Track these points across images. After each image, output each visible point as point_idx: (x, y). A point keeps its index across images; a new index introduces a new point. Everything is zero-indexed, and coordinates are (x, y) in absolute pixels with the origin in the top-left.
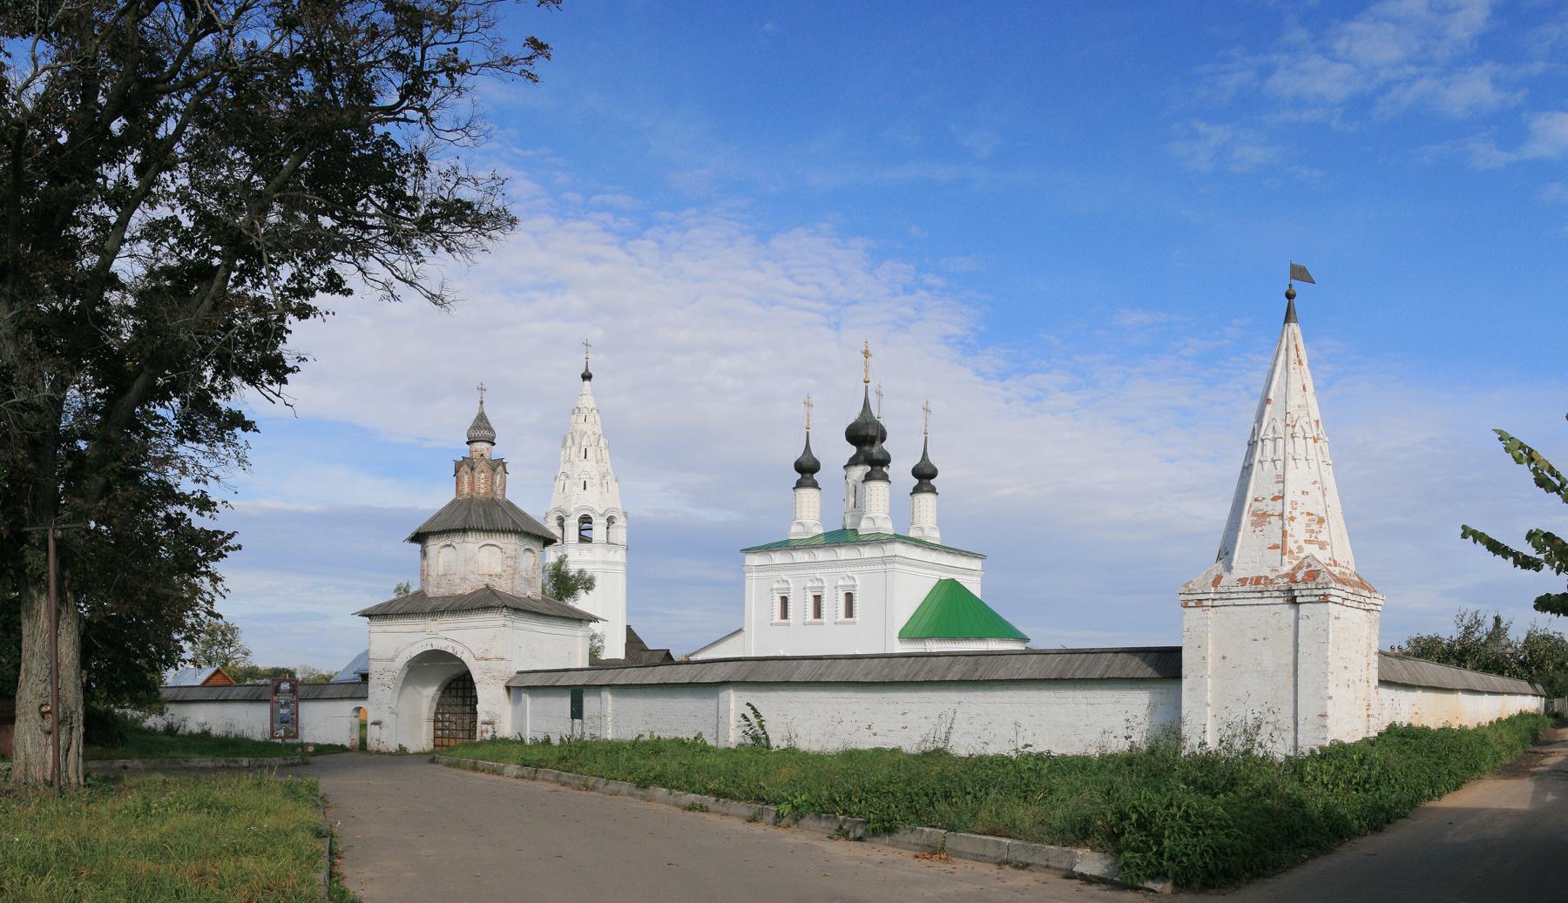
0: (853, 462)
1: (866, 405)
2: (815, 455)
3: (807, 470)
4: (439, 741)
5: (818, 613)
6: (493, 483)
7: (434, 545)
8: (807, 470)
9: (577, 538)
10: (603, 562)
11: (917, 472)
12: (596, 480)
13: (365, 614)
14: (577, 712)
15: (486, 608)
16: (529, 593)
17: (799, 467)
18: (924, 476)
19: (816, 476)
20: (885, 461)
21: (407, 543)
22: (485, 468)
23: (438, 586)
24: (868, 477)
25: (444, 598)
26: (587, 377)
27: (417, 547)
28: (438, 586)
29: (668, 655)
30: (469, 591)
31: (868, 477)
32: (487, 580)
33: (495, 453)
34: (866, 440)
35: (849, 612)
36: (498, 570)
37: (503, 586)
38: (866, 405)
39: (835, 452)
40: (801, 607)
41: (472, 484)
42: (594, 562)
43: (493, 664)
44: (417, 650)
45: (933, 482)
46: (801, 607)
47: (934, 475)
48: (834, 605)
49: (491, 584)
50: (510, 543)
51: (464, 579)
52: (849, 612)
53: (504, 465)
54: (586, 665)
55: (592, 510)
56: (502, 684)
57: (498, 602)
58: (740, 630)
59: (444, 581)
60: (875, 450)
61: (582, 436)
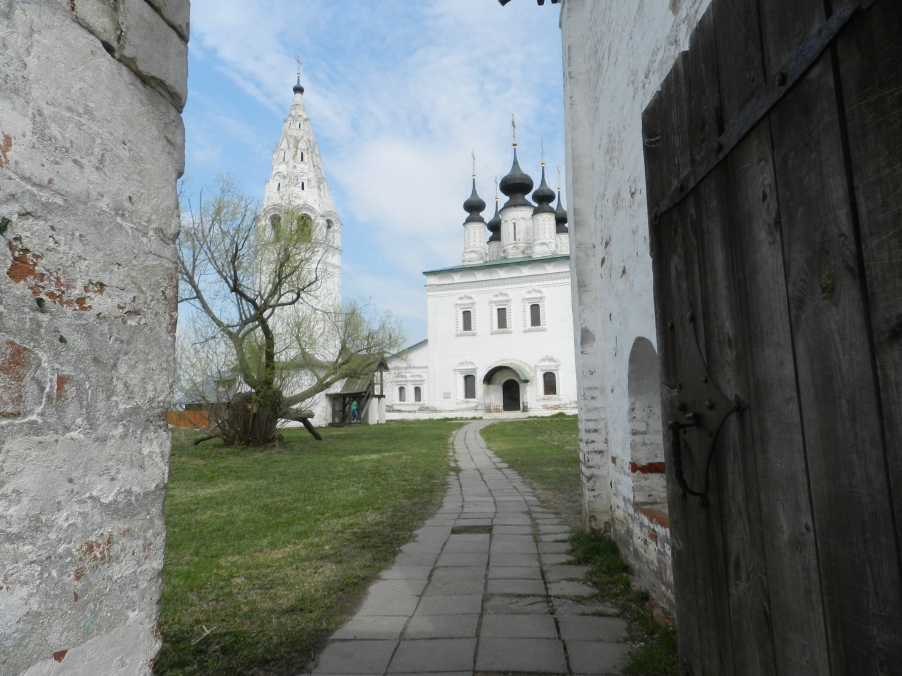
1: (515, 163)
40: (485, 319)
52: (536, 320)
55: (312, 209)
58: (425, 342)
61: (297, 142)
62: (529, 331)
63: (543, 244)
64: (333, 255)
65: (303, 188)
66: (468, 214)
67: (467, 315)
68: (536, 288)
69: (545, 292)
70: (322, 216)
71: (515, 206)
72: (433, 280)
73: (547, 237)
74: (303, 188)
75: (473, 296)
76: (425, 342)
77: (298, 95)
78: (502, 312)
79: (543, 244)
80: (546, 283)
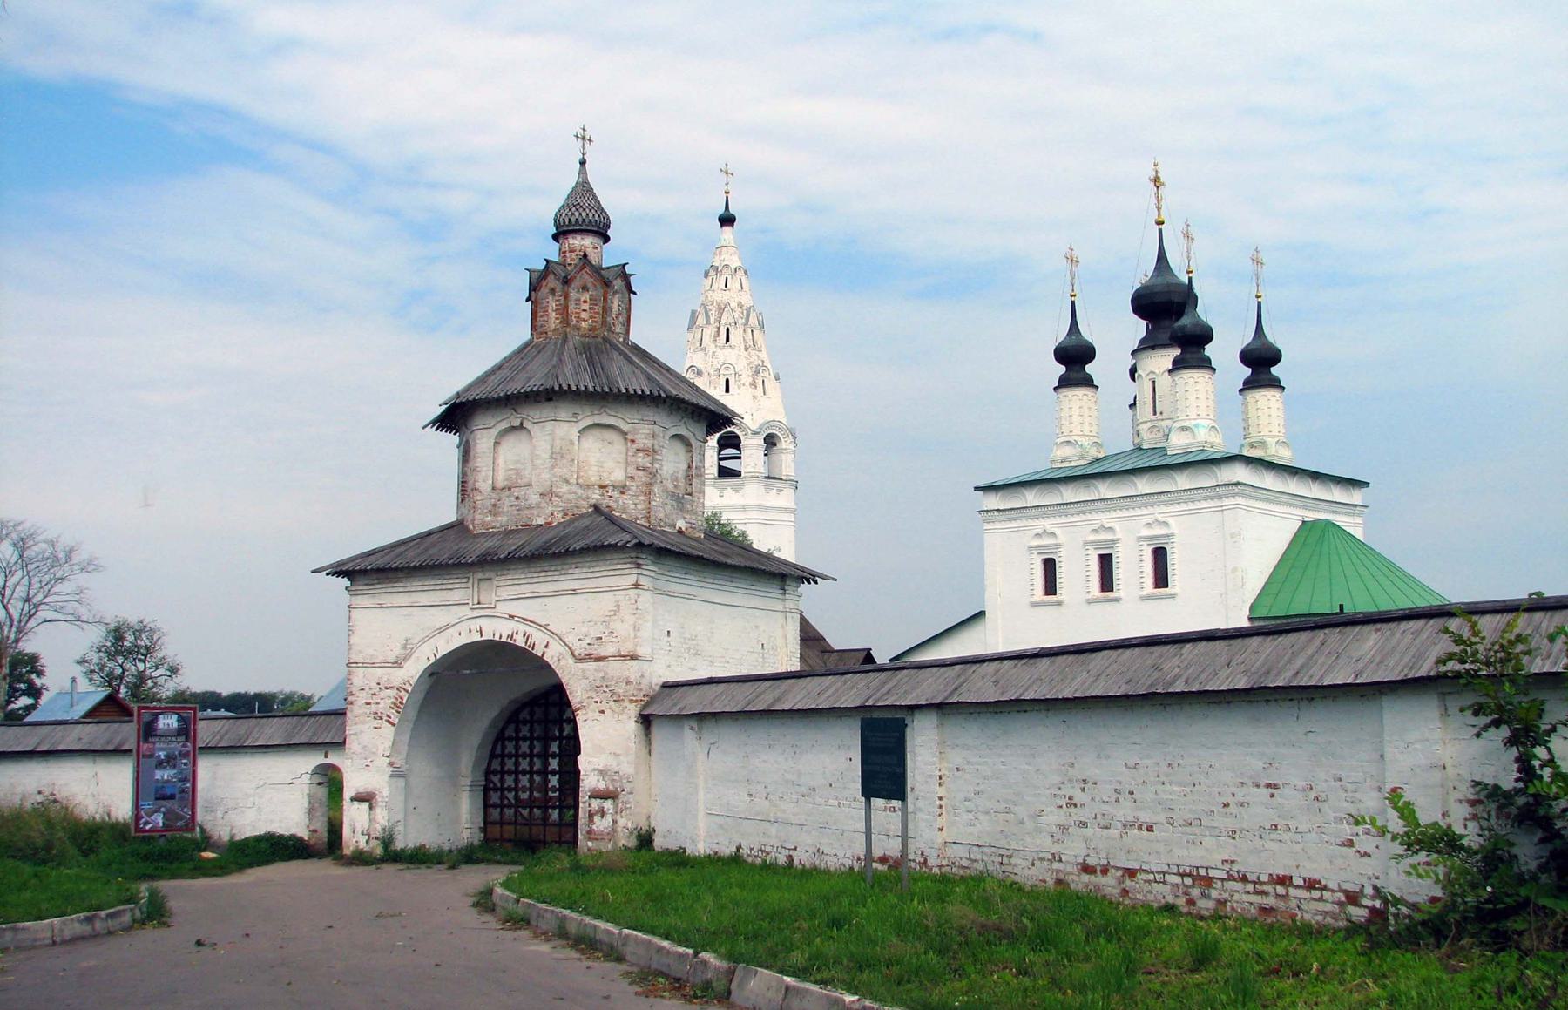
0: (1148, 344)
1: (1162, 257)
2: (1086, 333)
3: (1075, 359)
4: (495, 831)
5: (1107, 583)
6: (606, 310)
7: (484, 434)
8: (1075, 359)
9: (715, 471)
10: (761, 508)
11: (1247, 357)
12: (746, 378)
13: (339, 570)
14: (884, 775)
15: (597, 551)
16: (681, 524)
17: (1062, 355)
18: (1261, 363)
19: (1089, 368)
20: (1205, 336)
21: (431, 430)
22: (589, 281)
23: (495, 510)
24: (1178, 365)
25: (508, 533)
26: (727, 220)
27: (451, 440)
28: (495, 510)
29: (868, 658)
30: (559, 518)
31: (1178, 365)
32: (596, 496)
33: (609, 256)
34: (1168, 315)
35: (1161, 579)
36: (618, 476)
37: (629, 507)
38: (1162, 257)
39: (1116, 332)
40: (1078, 574)
41: (564, 311)
42: (744, 508)
43: (615, 669)
44: (447, 644)
45: (1274, 370)
46: (1078, 574)
47: (1275, 357)
48: (1133, 569)
49: (605, 502)
50: (645, 427)
51: (548, 494)
52: (1161, 579)
53: (626, 277)
54: (795, 666)
56: (633, 710)
57: (622, 538)
58: (981, 614)
59: (507, 501)
60: (1185, 321)
61: (721, 311)
62: (1148, 598)
63: (1184, 429)
64: (779, 491)
65: (727, 390)
66: (1062, 369)
67: (1050, 566)
68: (1160, 518)
69: (1175, 526)
70: (755, 433)
71: (1153, 348)
72: (993, 501)
73: (1192, 413)
74: (727, 390)
75: (1057, 531)
76: (981, 614)
77: (727, 229)
78: (1106, 562)
79: (1184, 429)
80: (1177, 508)
